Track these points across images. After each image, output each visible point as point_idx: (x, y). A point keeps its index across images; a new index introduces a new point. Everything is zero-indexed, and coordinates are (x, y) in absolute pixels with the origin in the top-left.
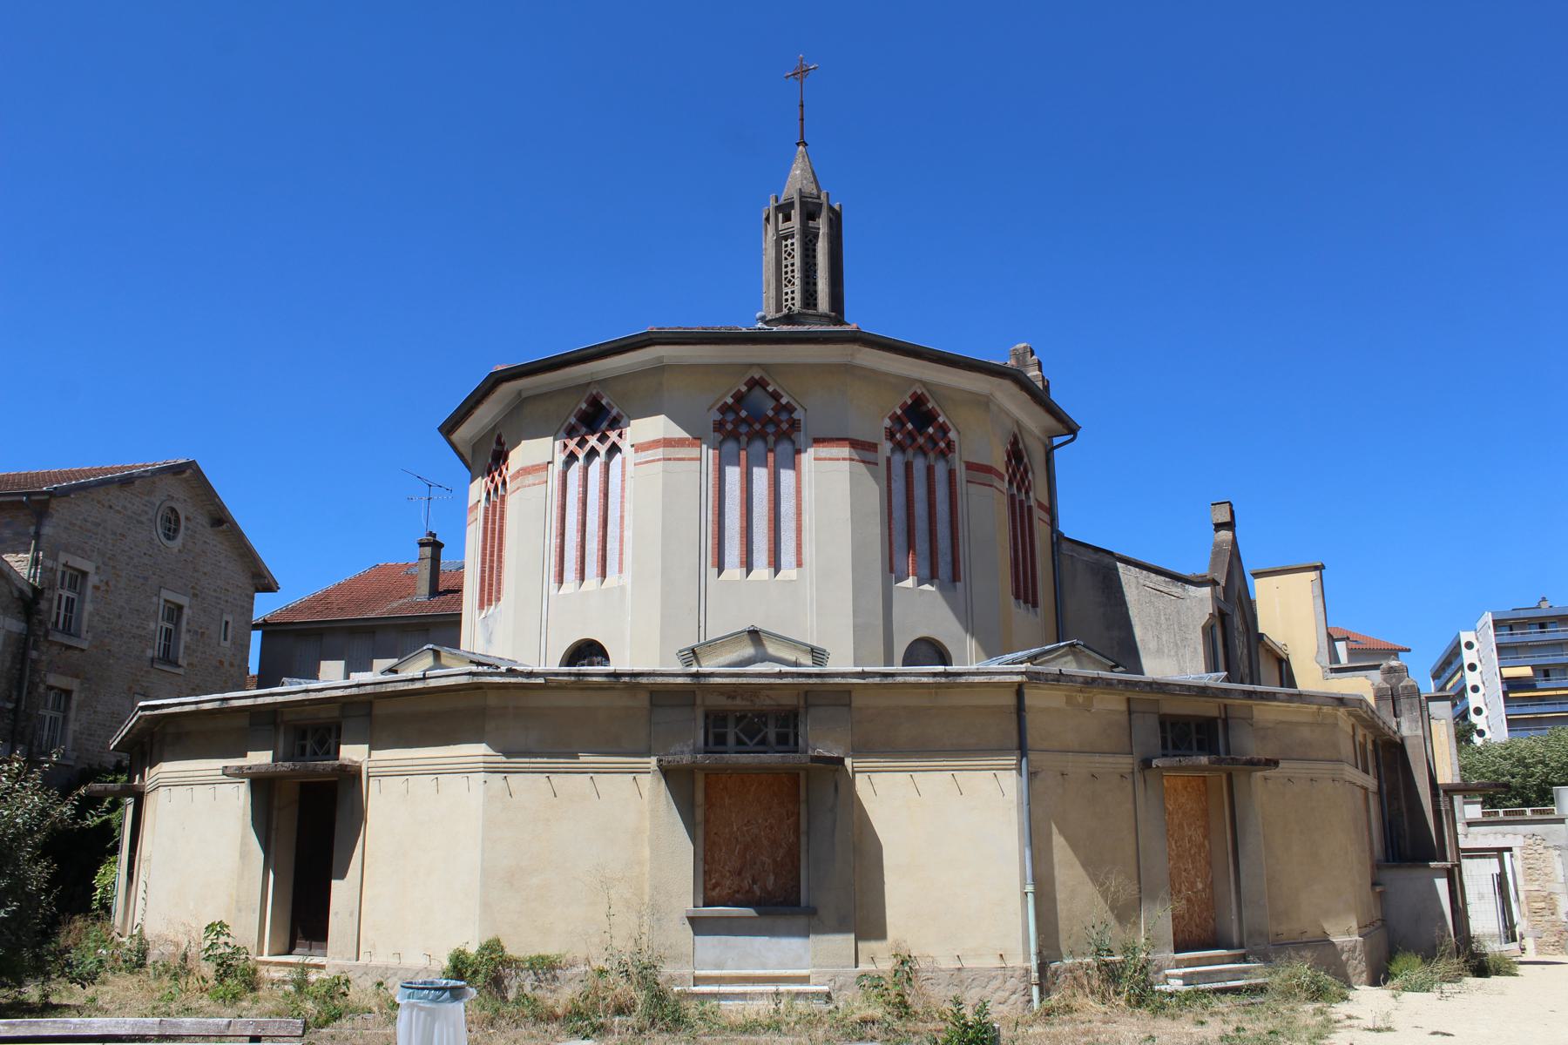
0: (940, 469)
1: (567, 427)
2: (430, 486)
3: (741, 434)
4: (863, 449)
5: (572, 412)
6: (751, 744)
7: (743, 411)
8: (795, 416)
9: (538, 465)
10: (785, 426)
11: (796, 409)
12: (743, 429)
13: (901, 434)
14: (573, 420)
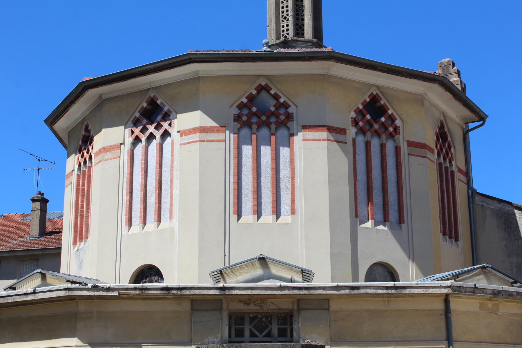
0: (390, 146)
1: (134, 119)
2: (39, 160)
3: (253, 123)
4: (335, 133)
5: (137, 108)
6: (261, 337)
8: (290, 110)
9: (114, 146)
10: (282, 118)
11: (290, 106)
12: (254, 120)
13: (363, 122)
14: (137, 115)
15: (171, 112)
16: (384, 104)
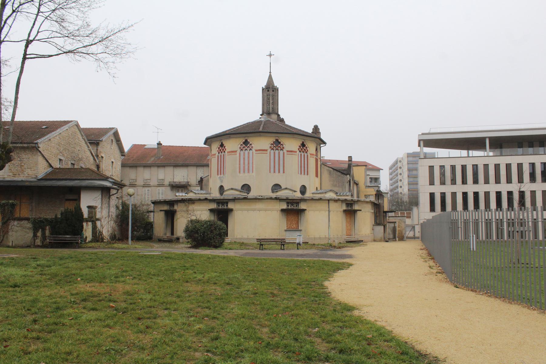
0: (306, 154)
8: (283, 146)
10: (282, 148)
12: (275, 148)
14: (242, 143)
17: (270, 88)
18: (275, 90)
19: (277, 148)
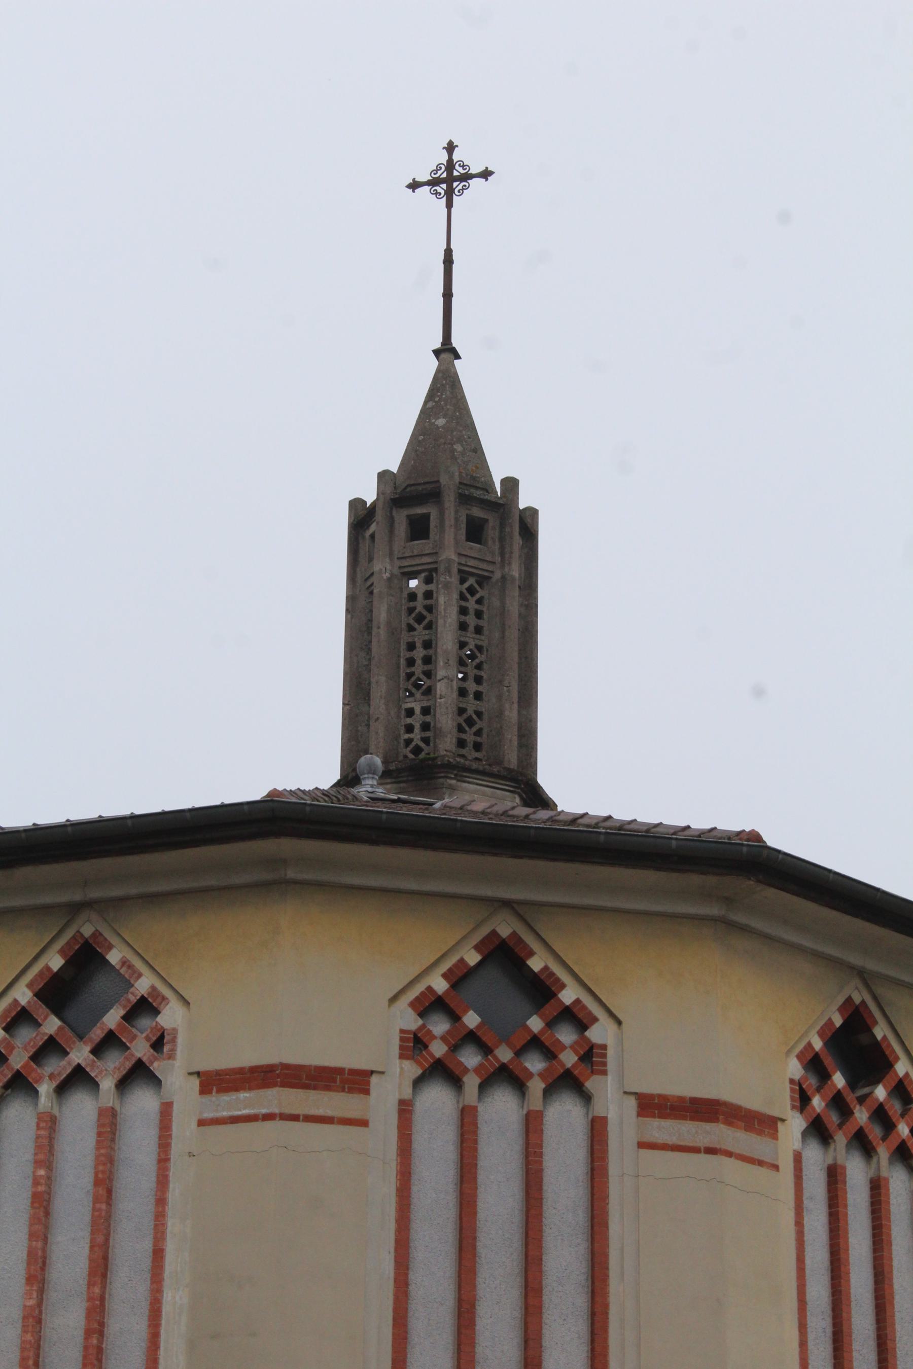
7: (471, 1012)
8: (595, 1034)
10: (569, 1059)
11: (595, 1020)
12: (470, 1058)
14: (23, 995)
15: (164, 998)
16: (885, 1038)
17: (434, 495)
18: (493, 521)
19: (504, 1054)
